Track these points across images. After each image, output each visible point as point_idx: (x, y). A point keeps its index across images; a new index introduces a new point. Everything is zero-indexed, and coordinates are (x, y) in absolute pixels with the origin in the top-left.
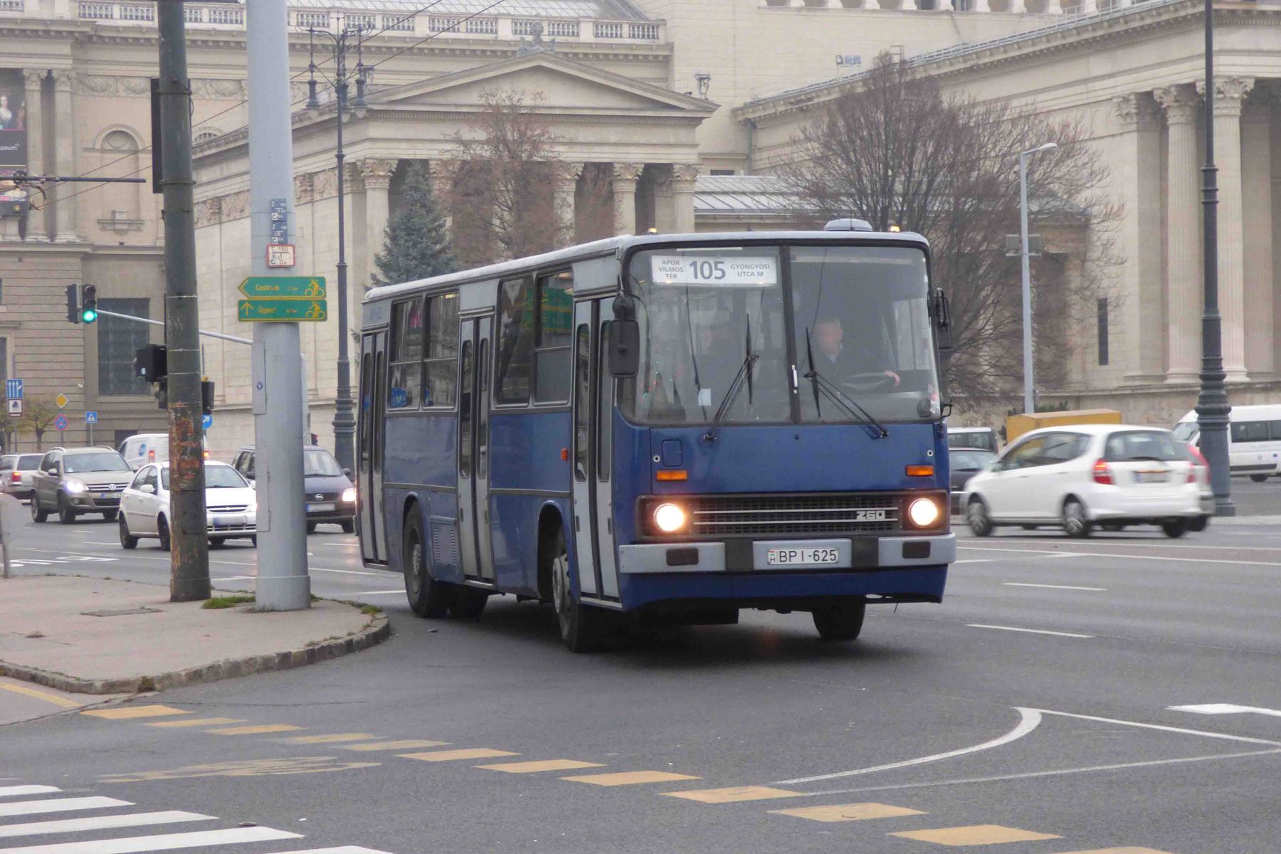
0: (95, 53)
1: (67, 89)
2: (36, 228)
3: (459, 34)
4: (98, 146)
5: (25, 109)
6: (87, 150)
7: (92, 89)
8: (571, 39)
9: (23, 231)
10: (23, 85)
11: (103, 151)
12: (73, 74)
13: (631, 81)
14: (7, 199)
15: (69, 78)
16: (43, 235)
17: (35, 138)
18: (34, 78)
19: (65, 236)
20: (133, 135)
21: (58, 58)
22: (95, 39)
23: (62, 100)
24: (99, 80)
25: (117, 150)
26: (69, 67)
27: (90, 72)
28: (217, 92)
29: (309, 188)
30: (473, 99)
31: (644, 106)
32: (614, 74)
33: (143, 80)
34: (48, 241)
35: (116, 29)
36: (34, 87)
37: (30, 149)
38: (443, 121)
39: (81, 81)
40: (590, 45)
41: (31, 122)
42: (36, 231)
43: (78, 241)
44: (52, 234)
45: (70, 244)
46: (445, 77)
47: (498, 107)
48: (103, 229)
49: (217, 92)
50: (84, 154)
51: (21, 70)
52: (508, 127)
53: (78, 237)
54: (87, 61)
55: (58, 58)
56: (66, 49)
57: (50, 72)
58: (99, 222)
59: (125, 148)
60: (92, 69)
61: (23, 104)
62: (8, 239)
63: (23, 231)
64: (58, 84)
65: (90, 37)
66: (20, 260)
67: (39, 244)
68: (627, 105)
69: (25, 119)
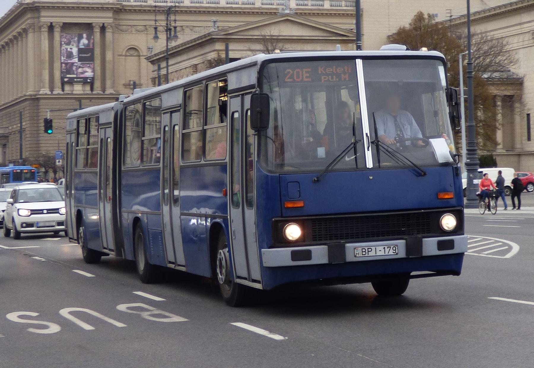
0: (123, 16)
1: (111, 31)
2: (97, 88)
3: (273, 6)
4: (124, 54)
5: (93, 39)
6: (119, 55)
7: (121, 30)
8: (321, 8)
9: (92, 89)
10: (93, 29)
11: (126, 56)
12: (113, 25)
13: (325, 24)
14: (86, 76)
15: (111, 26)
16: (100, 90)
17: (97, 51)
18: (97, 27)
19: (109, 91)
20: (139, 50)
21: (107, 18)
22: (123, 11)
23: (109, 35)
24: (124, 27)
25: (131, 56)
26: (111, 22)
27: (121, 24)
29: (195, 70)
30: (256, 33)
31: (332, 35)
32: (315, 21)
33: (143, 27)
34: (102, 93)
35: (131, 6)
36: (97, 31)
37: (95, 55)
38: (246, 42)
39: (117, 28)
40: (328, 10)
41: (95, 45)
42: (98, 90)
43: (114, 93)
44: (104, 89)
45: (111, 94)
46: (248, 23)
47: (265, 36)
48: (126, 88)
49: (136, 30)
50: (119, 57)
51: (92, 23)
52: (269, 44)
53: (115, 91)
54: (119, 19)
55: (107, 18)
57: (103, 24)
58: (124, 85)
59: (135, 55)
60: (122, 22)
61: (92, 37)
62: (86, 92)
63: (92, 89)
64: (107, 29)
65: (121, 9)
66: (91, 101)
67: (98, 94)
68: (325, 35)
69: (93, 44)
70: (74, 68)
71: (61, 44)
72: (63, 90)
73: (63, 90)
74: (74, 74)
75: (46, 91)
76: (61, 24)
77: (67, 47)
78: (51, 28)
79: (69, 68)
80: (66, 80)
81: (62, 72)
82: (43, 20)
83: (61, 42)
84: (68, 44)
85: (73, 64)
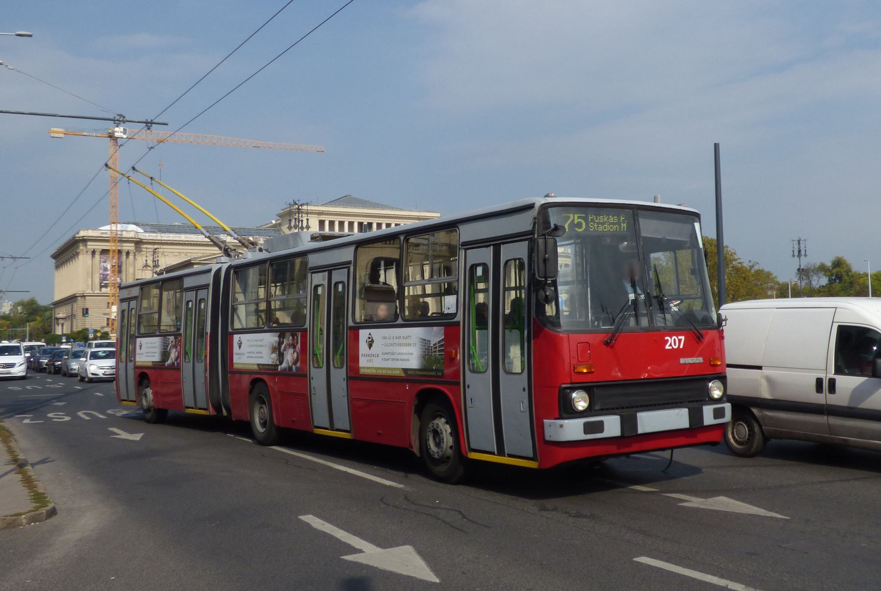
6: (138, 270)
11: (142, 270)
28: (174, 255)
55: (130, 247)
56: (133, 245)
57: (128, 250)
70: (108, 277)
71: (100, 262)
72: (100, 291)
73: (100, 291)
74: (108, 281)
75: (89, 291)
76: (101, 250)
77: (104, 264)
78: (94, 252)
79: (104, 277)
80: (103, 284)
81: (100, 280)
82: (88, 247)
83: (100, 261)
84: (105, 262)
85: (107, 275)
